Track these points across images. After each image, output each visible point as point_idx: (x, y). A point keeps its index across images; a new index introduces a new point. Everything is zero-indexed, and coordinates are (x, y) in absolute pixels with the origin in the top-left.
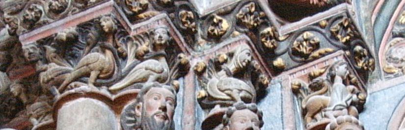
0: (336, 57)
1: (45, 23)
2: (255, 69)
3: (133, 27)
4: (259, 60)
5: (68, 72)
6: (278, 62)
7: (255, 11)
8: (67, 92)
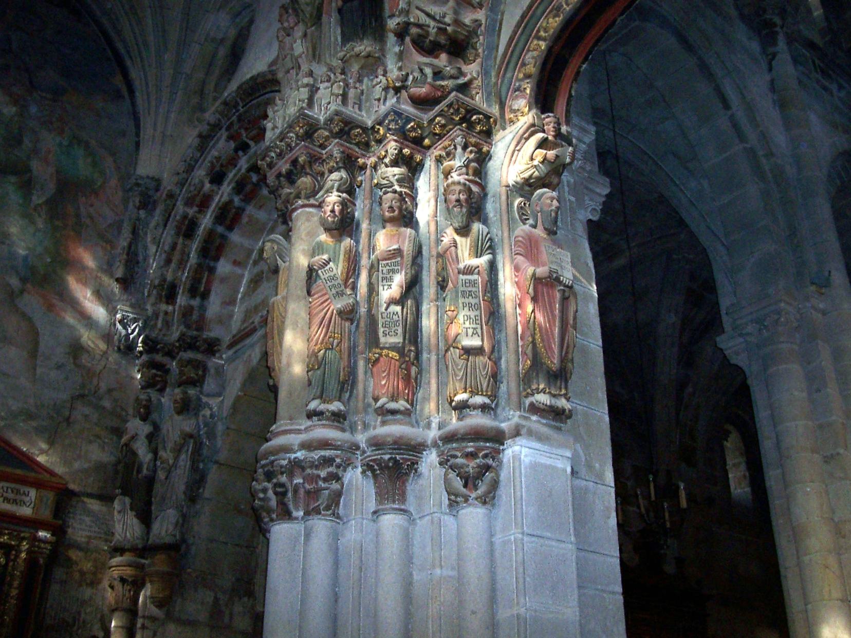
0: (456, 131)
1: (276, 164)
3: (324, 152)
5: (291, 193)
6: (427, 142)
8: (294, 207)
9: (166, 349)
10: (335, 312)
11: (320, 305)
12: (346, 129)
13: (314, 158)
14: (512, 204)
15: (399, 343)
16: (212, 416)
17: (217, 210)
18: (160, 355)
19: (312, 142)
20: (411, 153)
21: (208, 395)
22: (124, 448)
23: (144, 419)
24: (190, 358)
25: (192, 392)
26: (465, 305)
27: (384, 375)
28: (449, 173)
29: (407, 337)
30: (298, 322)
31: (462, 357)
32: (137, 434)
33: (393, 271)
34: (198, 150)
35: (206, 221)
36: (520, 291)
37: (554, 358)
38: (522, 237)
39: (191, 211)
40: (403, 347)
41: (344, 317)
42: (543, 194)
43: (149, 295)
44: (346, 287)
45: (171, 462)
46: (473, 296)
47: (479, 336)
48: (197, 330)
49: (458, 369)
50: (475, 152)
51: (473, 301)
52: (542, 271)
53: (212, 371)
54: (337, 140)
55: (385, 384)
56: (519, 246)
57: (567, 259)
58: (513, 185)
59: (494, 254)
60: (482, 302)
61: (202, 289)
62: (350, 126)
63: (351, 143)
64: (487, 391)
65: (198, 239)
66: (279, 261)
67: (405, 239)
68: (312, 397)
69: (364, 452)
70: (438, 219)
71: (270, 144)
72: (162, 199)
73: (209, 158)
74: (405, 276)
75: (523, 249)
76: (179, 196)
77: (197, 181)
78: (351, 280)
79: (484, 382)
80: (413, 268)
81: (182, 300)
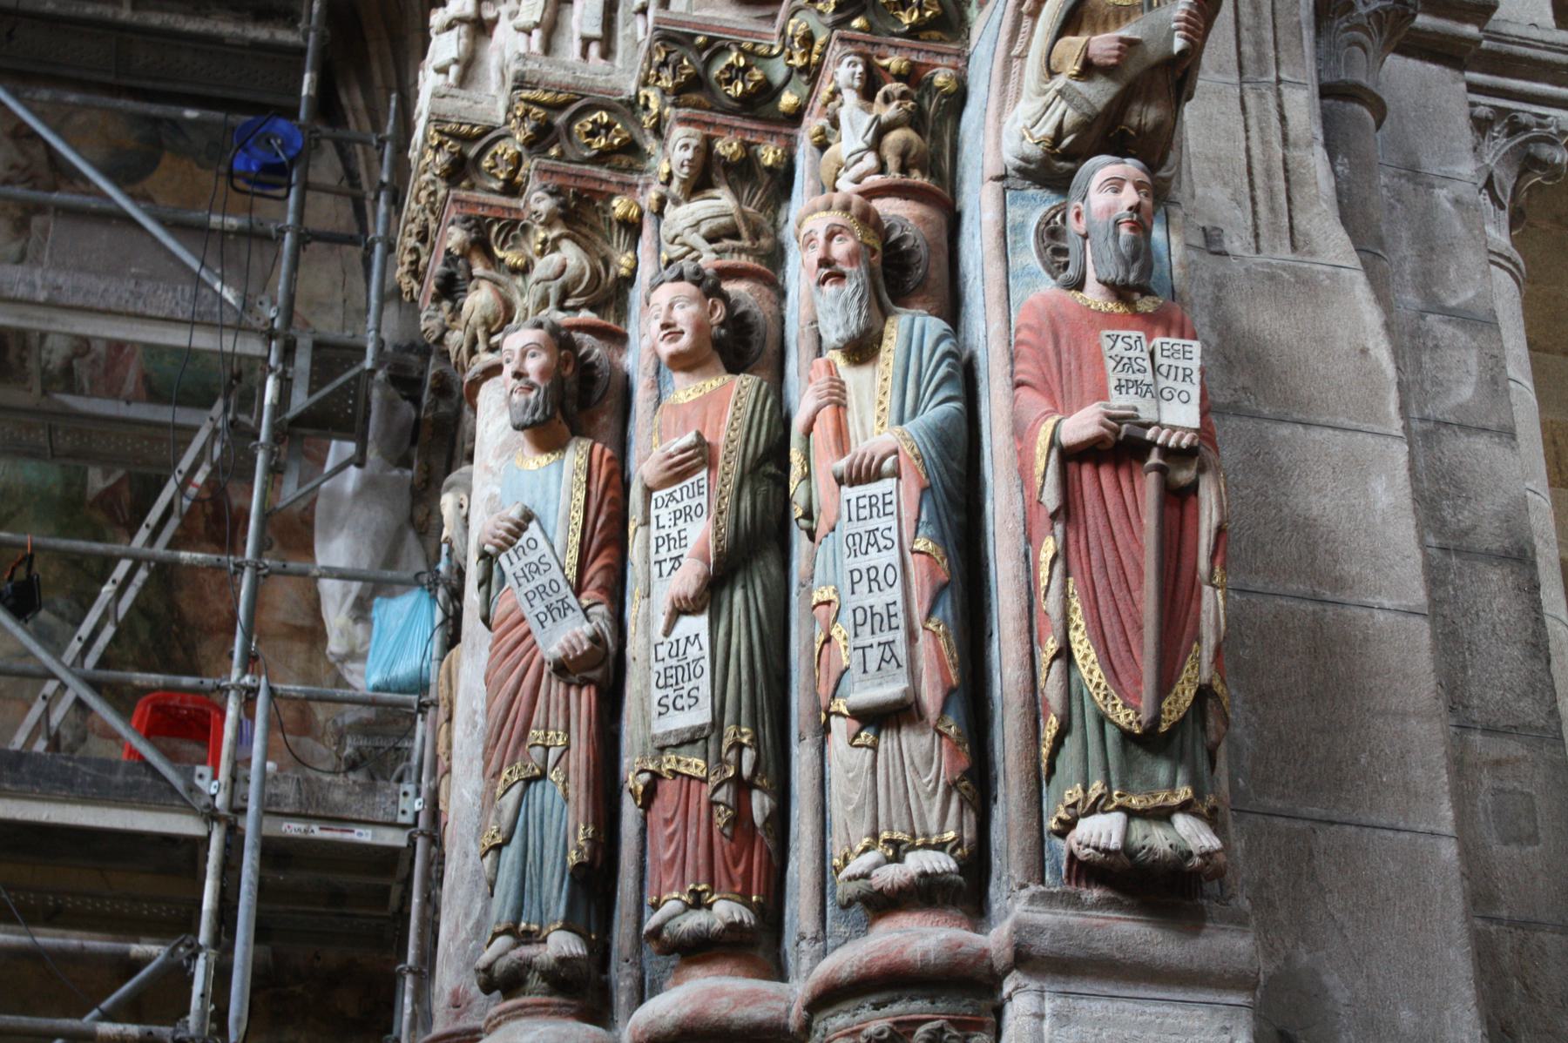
2: (724, 157)
4: (730, 128)
6: (788, 100)
7: (668, 54)
10: (547, 669)
11: (507, 654)
12: (560, 119)
14: (1020, 228)
15: (701, 728)
20: (746, 146)
31: (857, 742)
41: (576, 679)
46: (882, 542)
47: (899, 666)
51: (877, 559)
52: (1081, 425)
57: (1182, 364)
58: (1019, 170)
67: (721, 412)
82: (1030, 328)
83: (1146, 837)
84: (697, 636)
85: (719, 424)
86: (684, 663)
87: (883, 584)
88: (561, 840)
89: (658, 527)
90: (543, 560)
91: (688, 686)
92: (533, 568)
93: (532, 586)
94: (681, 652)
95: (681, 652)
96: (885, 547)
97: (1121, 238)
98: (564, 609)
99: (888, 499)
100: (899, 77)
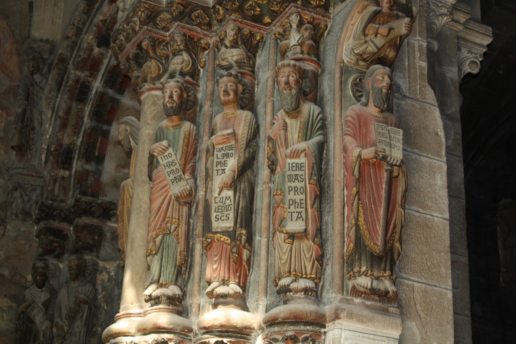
3: (168, 34)
5: (139, 77)
6: (267, 20)
9: (63, 215)
10: (173, 197)
13: (157, 42)
15: (230, 227)
16: (110, 279)
17: (106, 74)
18: (57, 221)
19: (156, 25)
21: (104, 260)
22: (22, 316)
23: (41, 286)
24: (86, 224)
25: (88, 257)
26: (291, 189)
27: (216, 259)
28: (286, 52)
29: (239, 221)
30: (141, 207)
32: (34, 302)
33: (227, 155)
34: (84, 13)
35: (97, 85)
36: (347, 171)
37: (378, 240)
38: (352, 117)
39: (82, 75)
40: (235, 231)
42: (376, 69)
43: (46, 161)
44: (184, 173)
45: (66, 328)
46: (300, 179)
48: (92, 195)
49: (282, 253)
50: (310, 29)
51: (299, 185)
52: (368, 153)
53: (108, 235)
54: (177, 24)
55: (217, 268)
56: (348, 126)
57: (397, 136)
59: (325, 135)
60: (308, 185)
61: (97, 154)
62: (190, 7)
63: (193, 25)
64: (311, 274)
65: (91, 102)
66: (133, 143)
68: (150, 281)
69: (196, 335)
70: (275, 100)
71: (119, 27)
72: (54, 64)
73: (96, 21)
74: (238, 160)
75: (353, 130)
76: (70, 59)
77: (85, 45)
78: (191, 164)
79: (308, 267)
80: (247, 150)
81: (77, 165)
82: (352, 117)
83: (377, 285)
84: (230, 197)
85: (239, 127)
86: (224, 205)
87: (299, 193)
88: (175, 256)
89: (217, 158)
90: (174, 161)
91: (226, 213)
92: (170, 163)
93: (169, 170)
94: (224, 202)
95: (224, 202)
96: (301, 181)
97: (383, 93)
98: (181, 179)
99: (302, 165)
100: (309, 23)
